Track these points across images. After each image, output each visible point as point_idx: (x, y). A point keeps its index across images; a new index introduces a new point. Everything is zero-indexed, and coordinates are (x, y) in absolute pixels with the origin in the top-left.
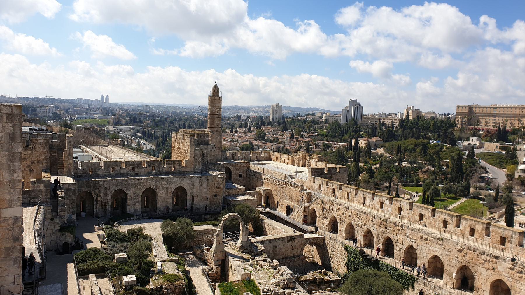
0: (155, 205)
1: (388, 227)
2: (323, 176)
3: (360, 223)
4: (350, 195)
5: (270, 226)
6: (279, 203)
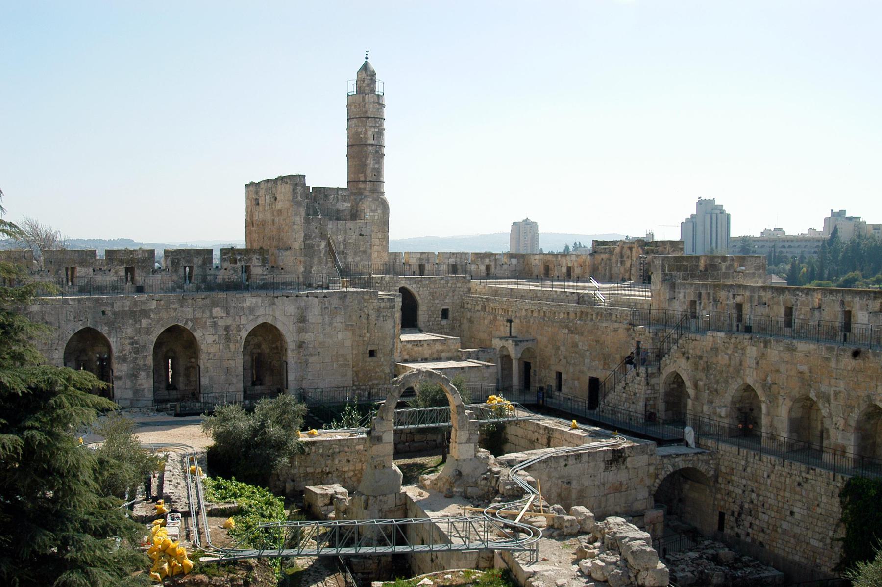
0: (196, 381)
3: (837, 389)
4: (795, 314)
5: (542, 431)
6: (564, 376)
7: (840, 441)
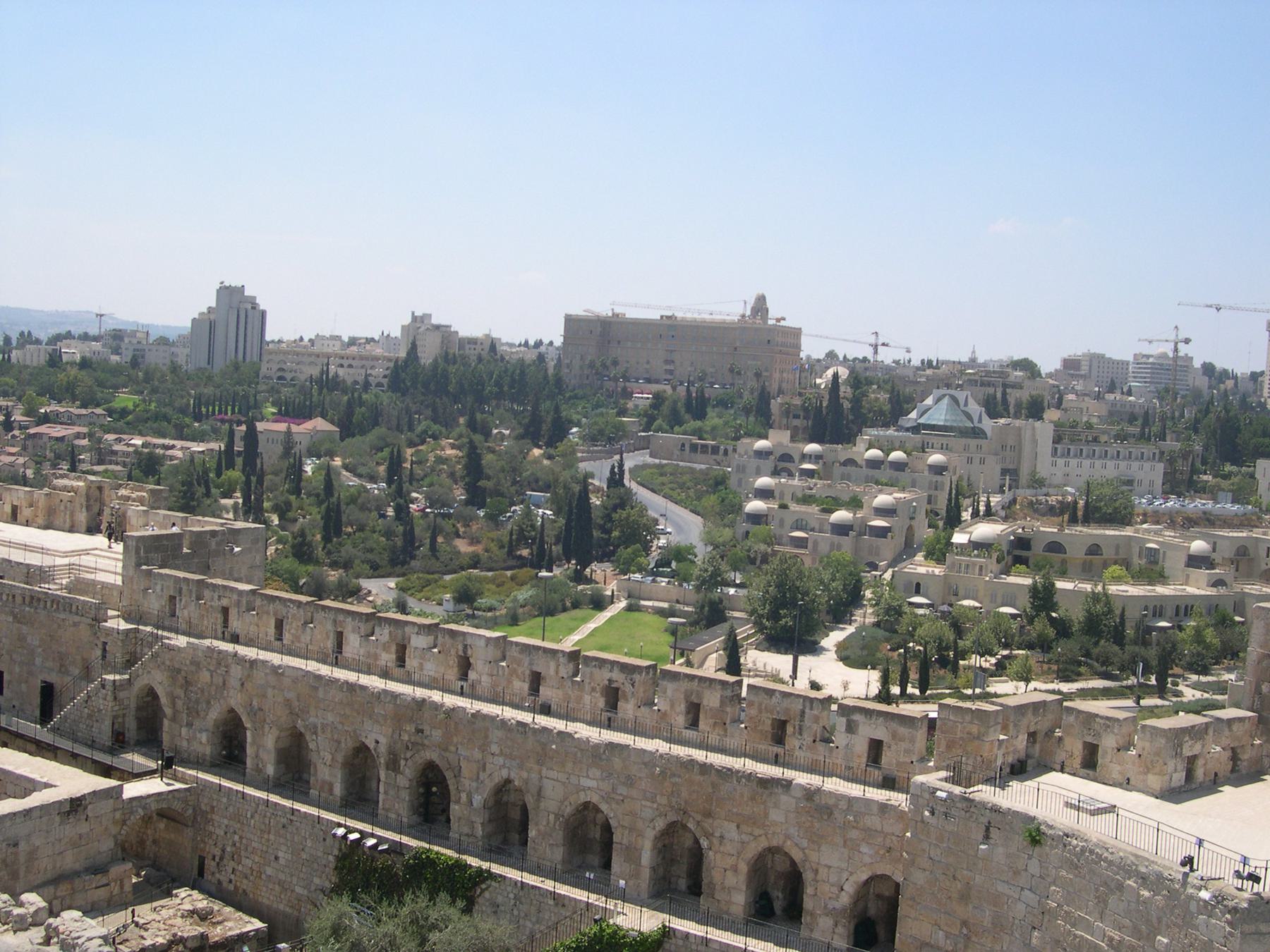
1: (426, 728)
2: (178, 562)
4: (286, 627)
7: (327, 778)
